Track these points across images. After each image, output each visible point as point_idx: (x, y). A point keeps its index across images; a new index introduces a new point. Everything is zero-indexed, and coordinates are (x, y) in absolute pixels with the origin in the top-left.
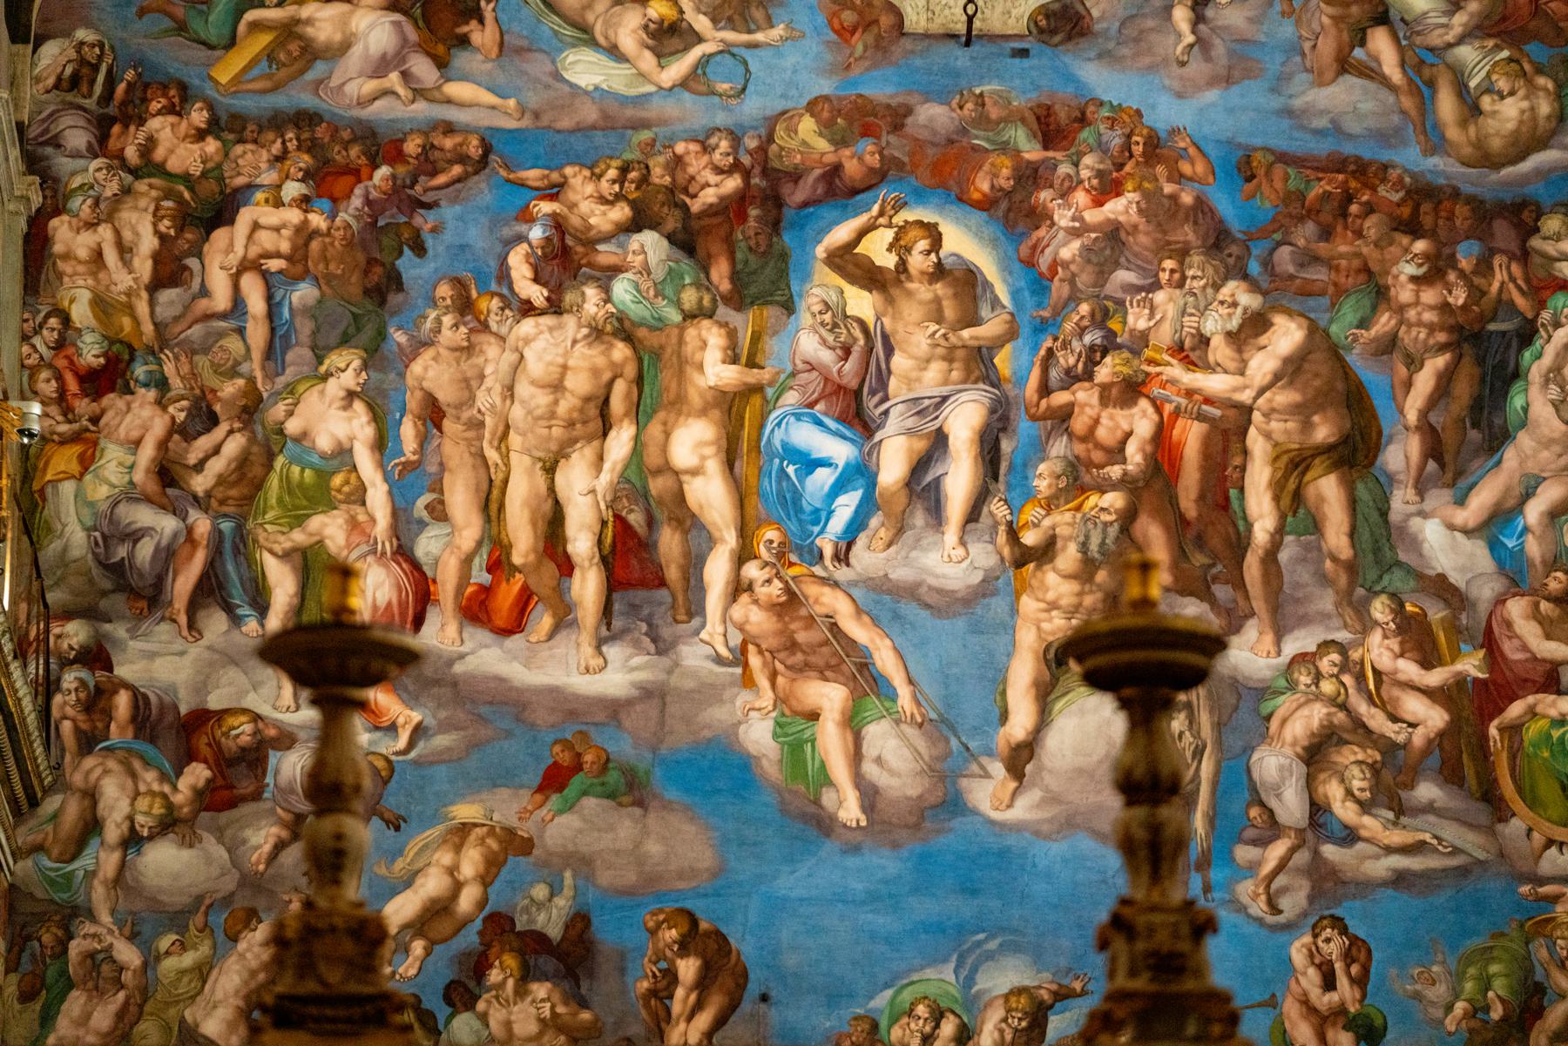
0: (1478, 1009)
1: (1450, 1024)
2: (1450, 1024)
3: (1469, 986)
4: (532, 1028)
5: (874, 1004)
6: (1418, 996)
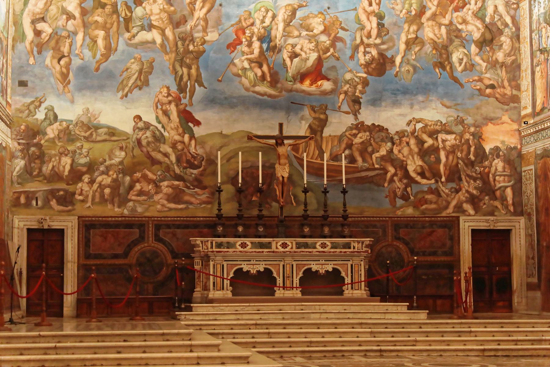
0: (409, 12)
1: (401, 16)
2: (401, 16)
3: (407, 6)
4: (158, 11)
5: (250, 7)
6: (393, 8)
